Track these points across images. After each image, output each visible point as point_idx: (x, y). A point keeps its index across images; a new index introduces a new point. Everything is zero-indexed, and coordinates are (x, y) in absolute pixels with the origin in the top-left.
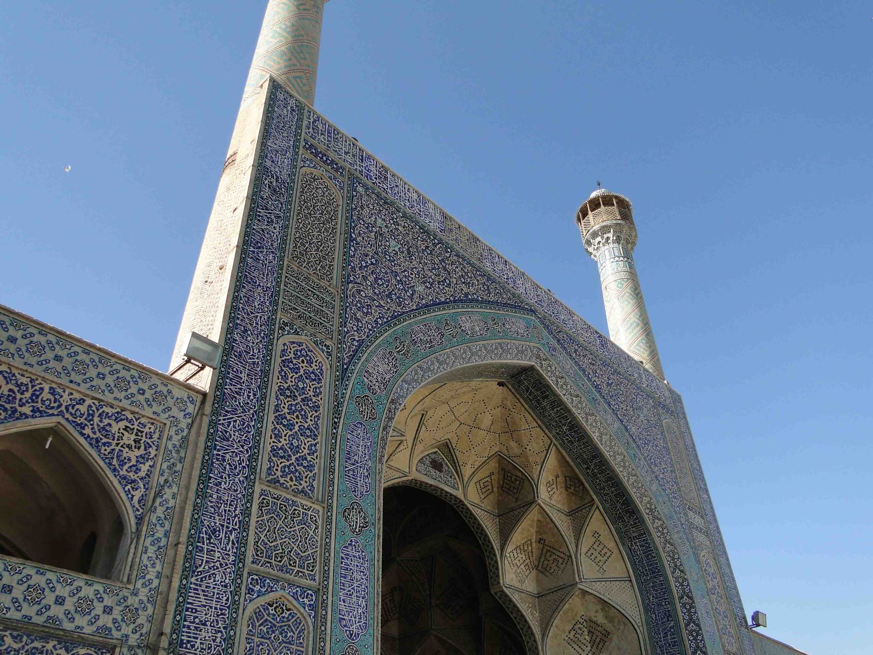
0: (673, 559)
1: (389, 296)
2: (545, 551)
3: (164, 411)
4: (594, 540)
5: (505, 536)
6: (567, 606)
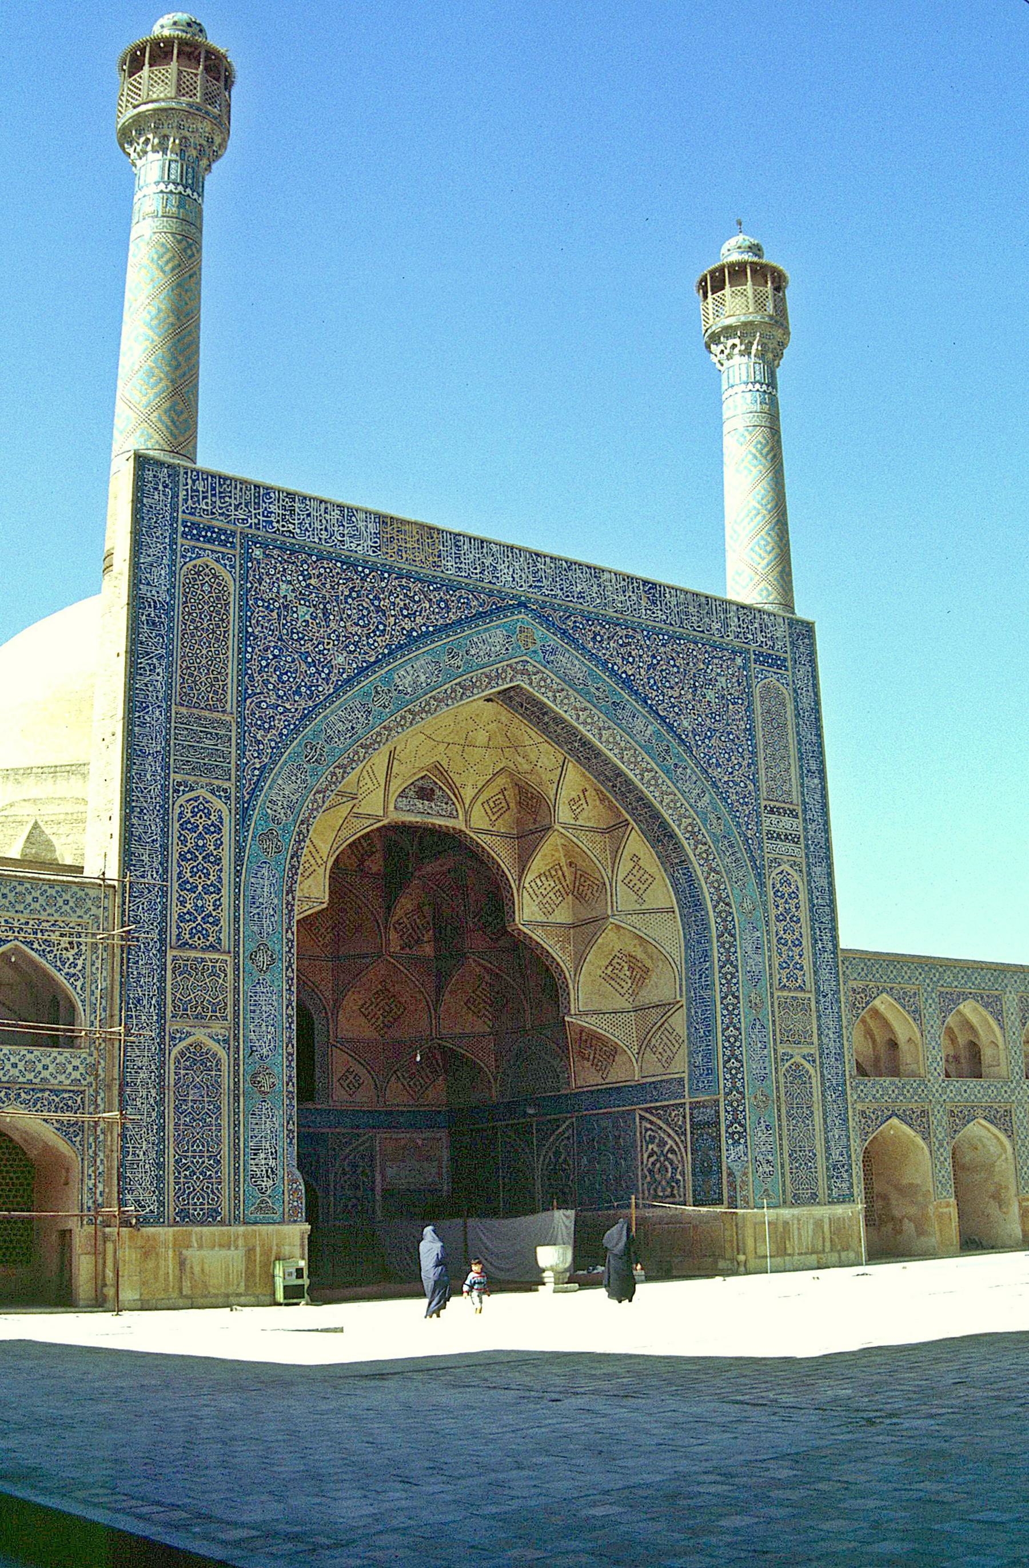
0: (717, 889)
1: (297, 692)
2: (578, 876)
3: (86, 913)
4: (633, 864)
5: (523, 863)
6: (600, 941)
